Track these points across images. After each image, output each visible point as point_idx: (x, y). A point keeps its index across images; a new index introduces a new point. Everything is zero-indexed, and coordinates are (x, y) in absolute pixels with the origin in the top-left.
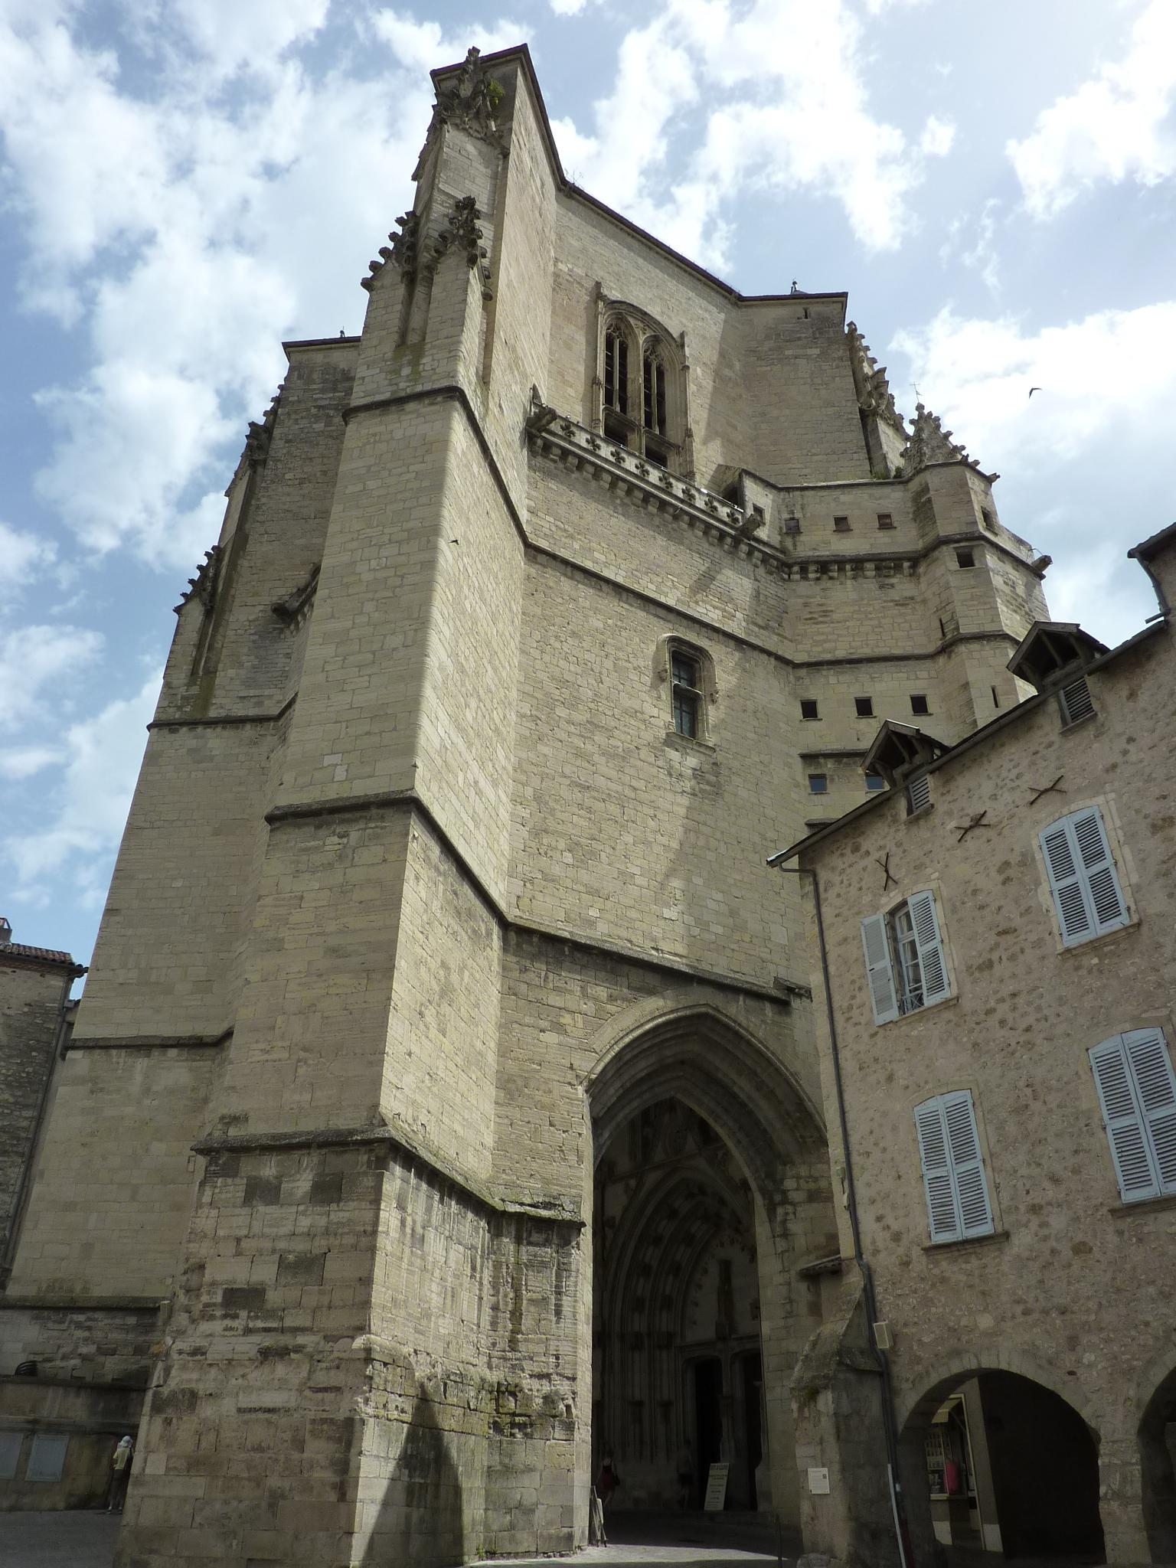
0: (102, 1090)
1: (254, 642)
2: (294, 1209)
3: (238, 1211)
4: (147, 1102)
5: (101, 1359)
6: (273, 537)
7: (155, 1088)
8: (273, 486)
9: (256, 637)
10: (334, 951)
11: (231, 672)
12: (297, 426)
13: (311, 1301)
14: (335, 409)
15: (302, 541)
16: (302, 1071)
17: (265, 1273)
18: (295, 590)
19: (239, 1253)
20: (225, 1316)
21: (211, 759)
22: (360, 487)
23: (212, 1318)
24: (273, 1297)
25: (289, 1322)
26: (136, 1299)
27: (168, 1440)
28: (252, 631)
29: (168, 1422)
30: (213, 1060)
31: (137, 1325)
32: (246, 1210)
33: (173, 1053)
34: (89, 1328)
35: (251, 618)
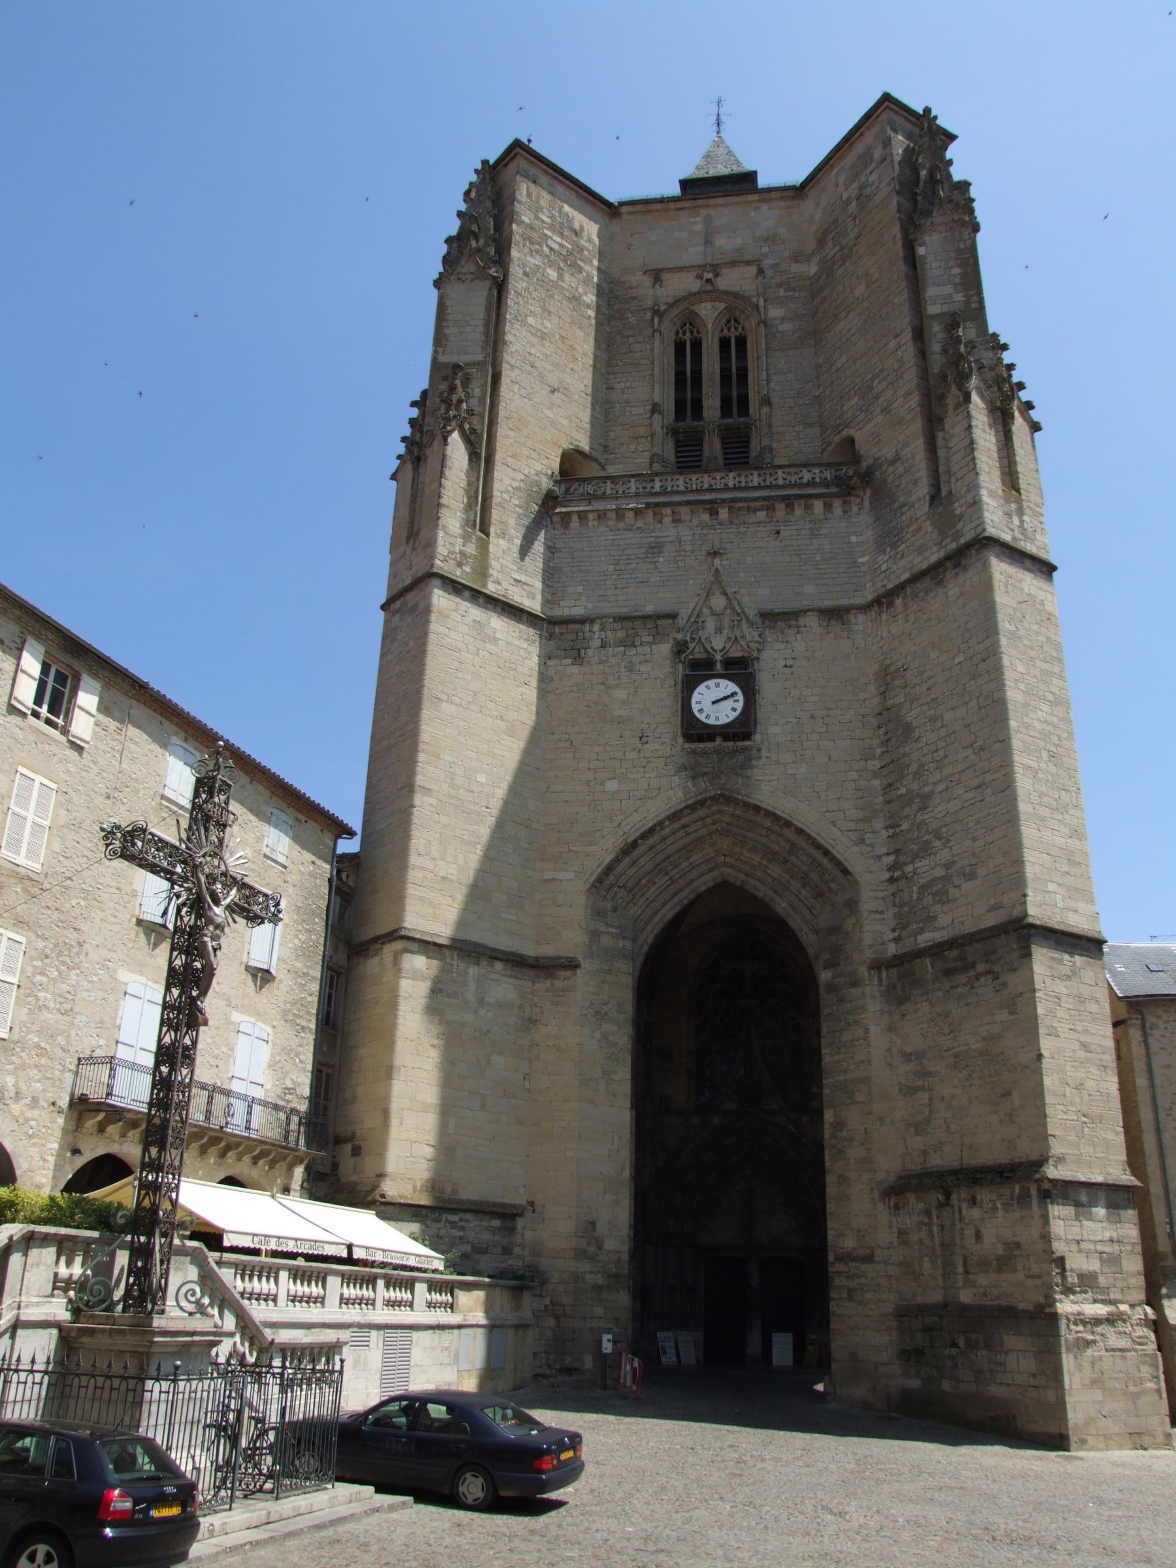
0: (441, 991)
1: (519, 515)
2: (1100, 1225)
3: (1073, 1223)
4: (482, 1012)
5: (477, 1256)
6: (524, 392)
7: (487, 999)
8: (517, 325)
9: (521, 511)
10: (1084, 1046)
11: (503, 543)
12: (532, 260)
13: (1120, 1284)
14: (565, 261)
15: (549, 413)
16: (1086, 1130)
17: (1094, 1265)
18: (549, 472)
19: (1080, 1251)
20: (1080, 1293)
21: (496, 640)
22: (1013, 628)
23: (1074, 1293)
24: (1102, 1280)
25: (1112, 1296)
26: (503, 1205)
27: (1080, 1367)
28: (517, 502)
29: (1076, 1357)
30: (534, 983)
31: (500, 1229)
32: (1077, 1223)
33: (499, 966)
34: (462, 1229)
35: (515, 484)
